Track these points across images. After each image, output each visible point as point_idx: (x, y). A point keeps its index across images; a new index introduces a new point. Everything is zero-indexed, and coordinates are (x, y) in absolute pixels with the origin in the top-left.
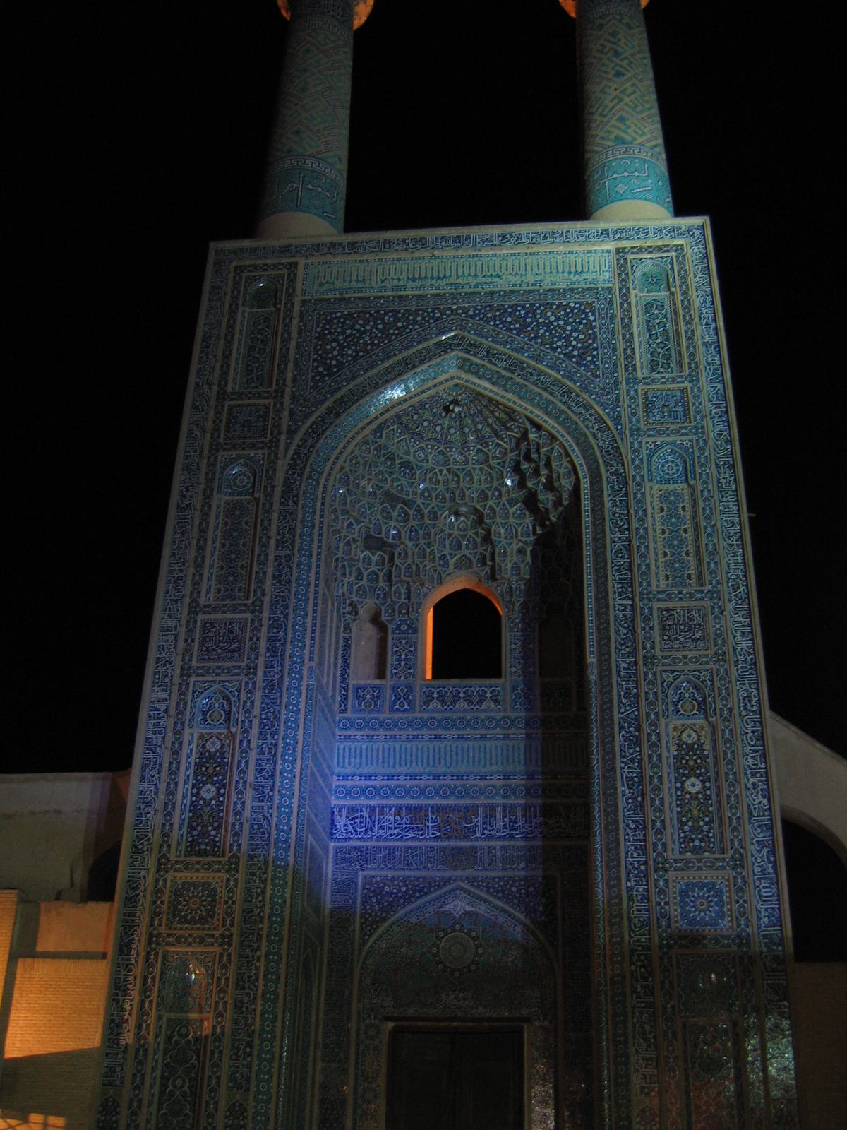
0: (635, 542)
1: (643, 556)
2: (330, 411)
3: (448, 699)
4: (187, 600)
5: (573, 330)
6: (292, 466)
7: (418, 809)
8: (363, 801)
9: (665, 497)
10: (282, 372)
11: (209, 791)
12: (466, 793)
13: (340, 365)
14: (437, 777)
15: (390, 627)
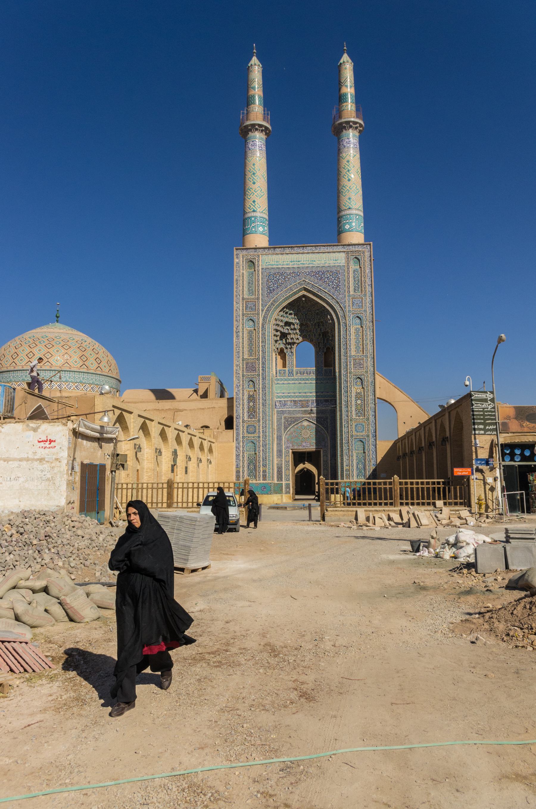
0: (348, 343)
1: (350, 346)
2: (272, 304)
3: (302, 373)
4: (241, 357)
5: (335, 279)
6: (264, 320)
7: (296, 401)
8: (282, 399)
9: (356, 329)
10: (258, 292)
11: (251, 404)
12: (307, 397)
13: (274, 290)
14: (300, 393)
15: (287, 354)
